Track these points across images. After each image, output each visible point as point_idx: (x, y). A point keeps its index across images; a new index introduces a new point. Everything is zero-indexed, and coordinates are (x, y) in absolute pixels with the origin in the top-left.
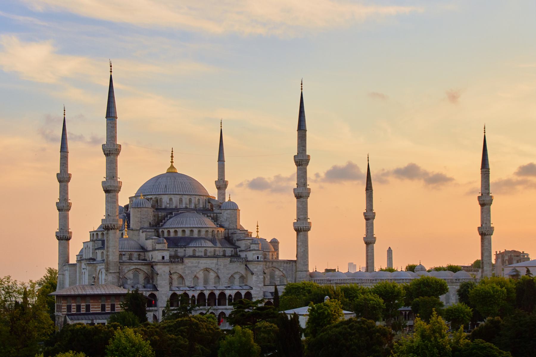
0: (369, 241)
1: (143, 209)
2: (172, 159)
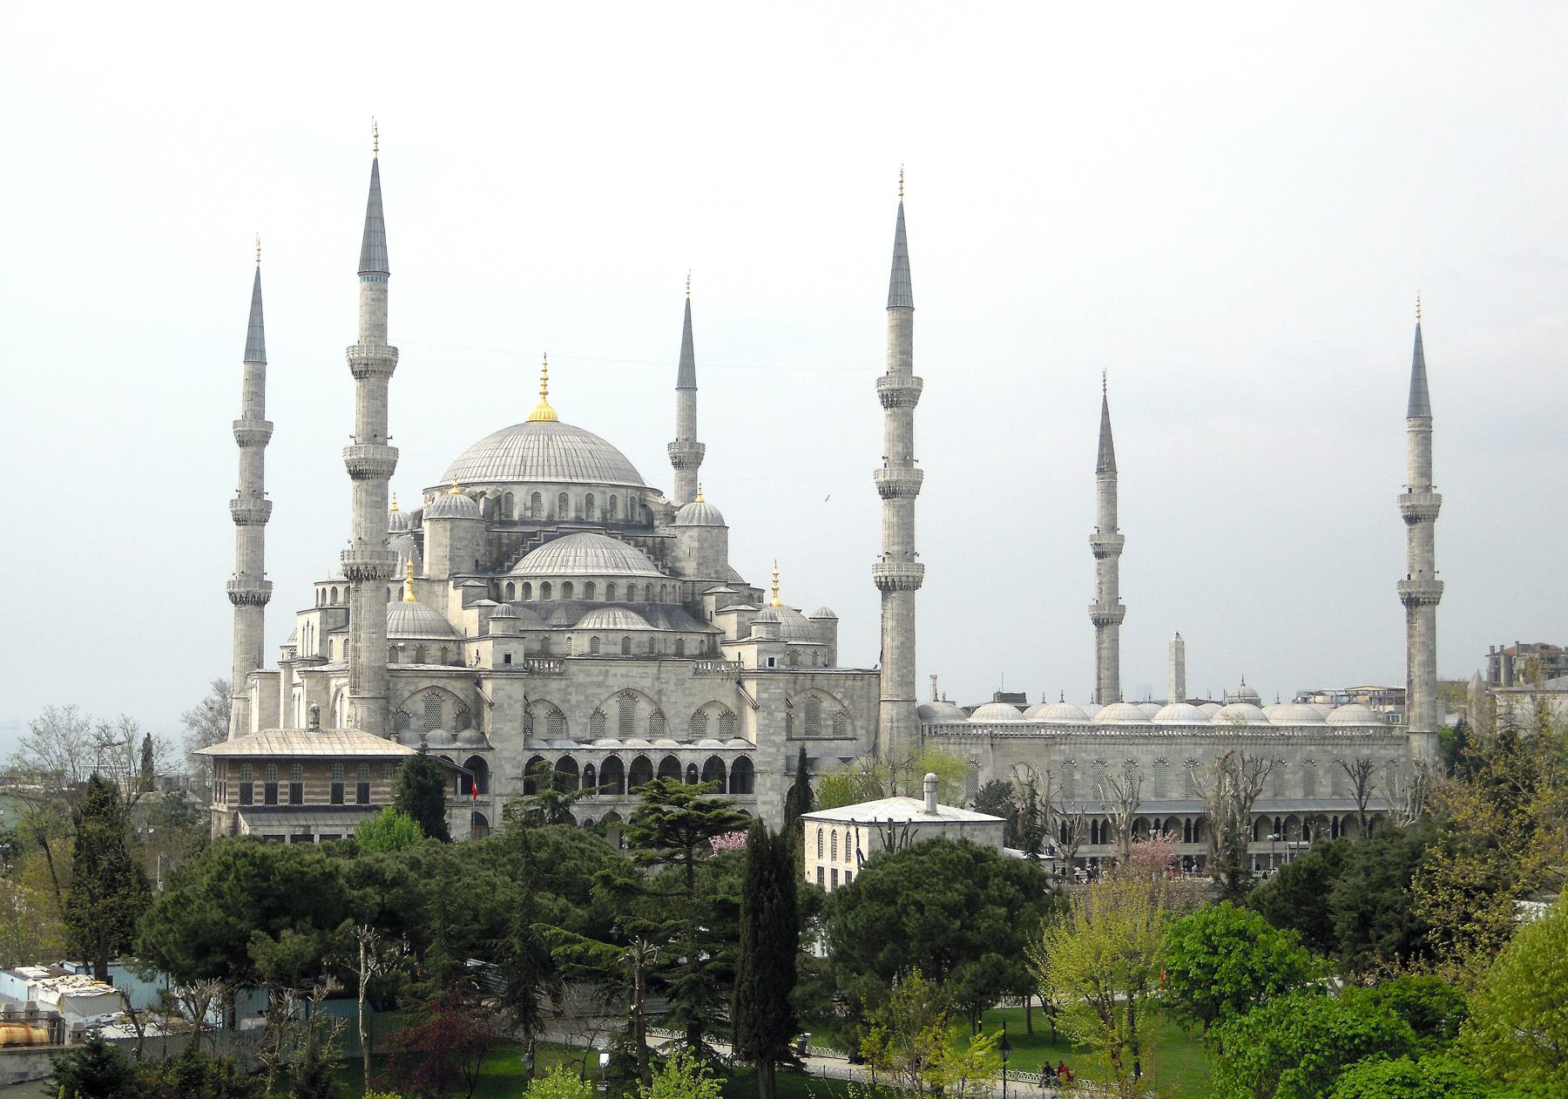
0: (1107, 620)
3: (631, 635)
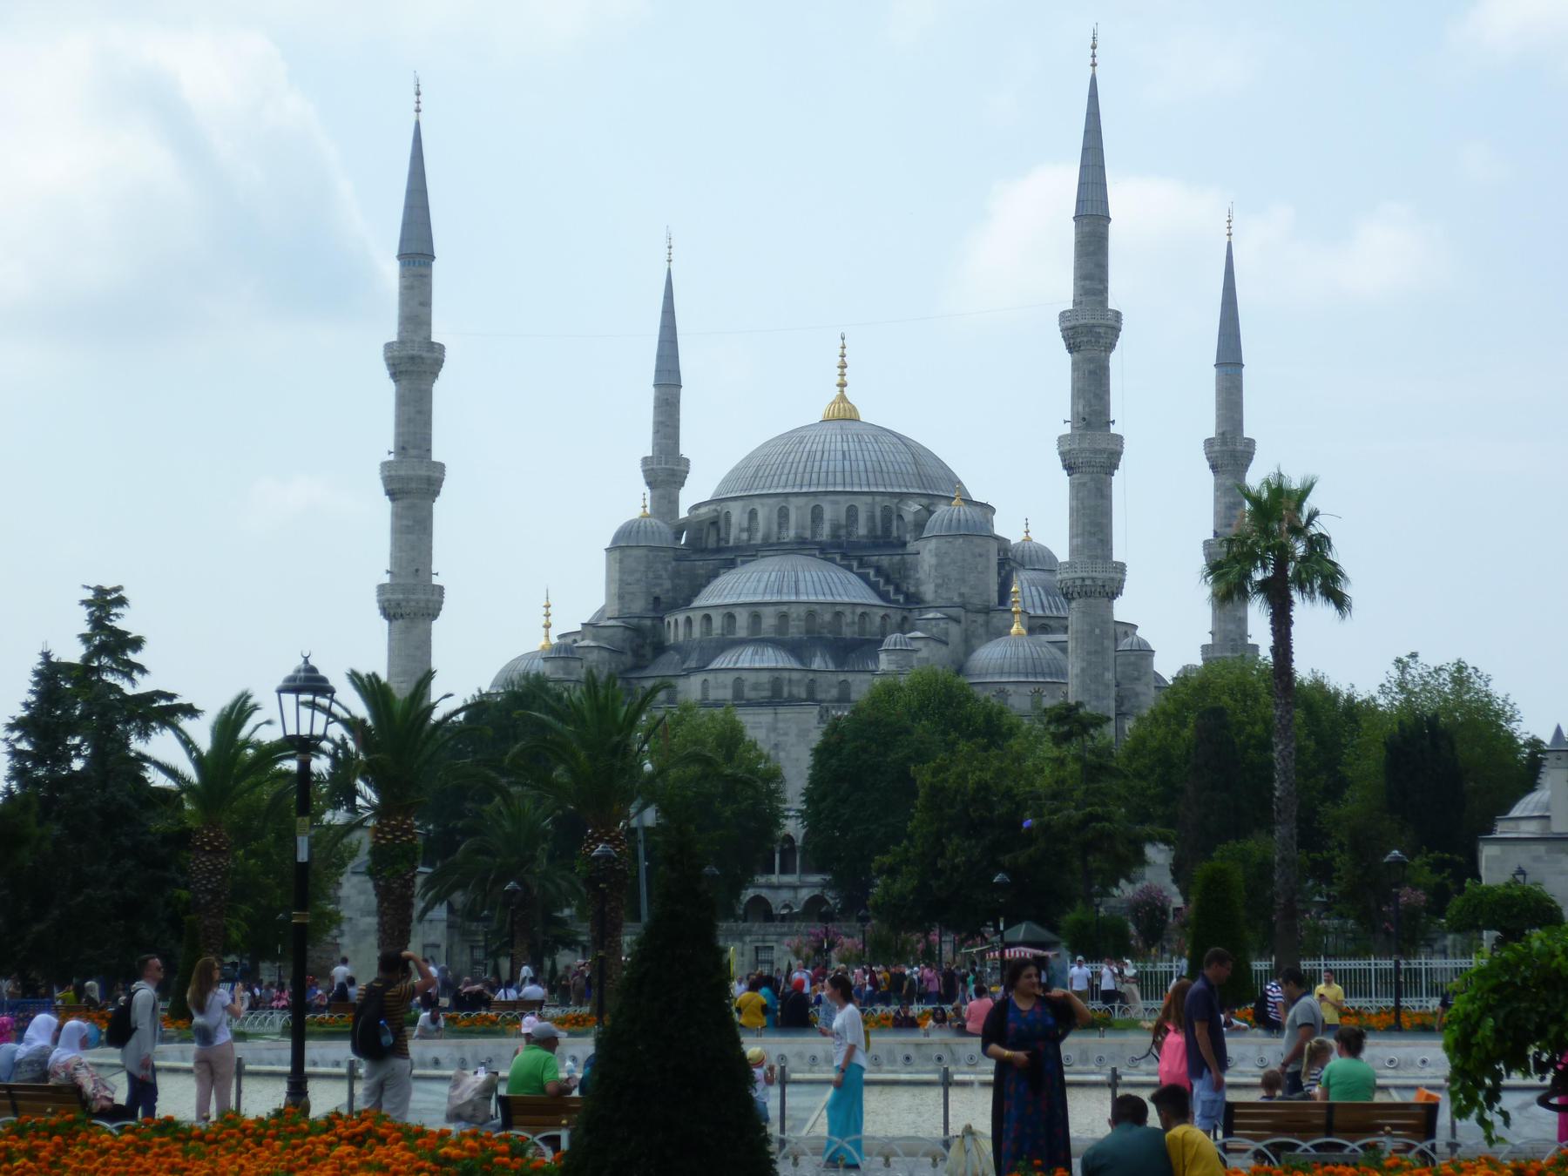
1: (628, 551)
2: (842, 375)
3: (744, 675)
